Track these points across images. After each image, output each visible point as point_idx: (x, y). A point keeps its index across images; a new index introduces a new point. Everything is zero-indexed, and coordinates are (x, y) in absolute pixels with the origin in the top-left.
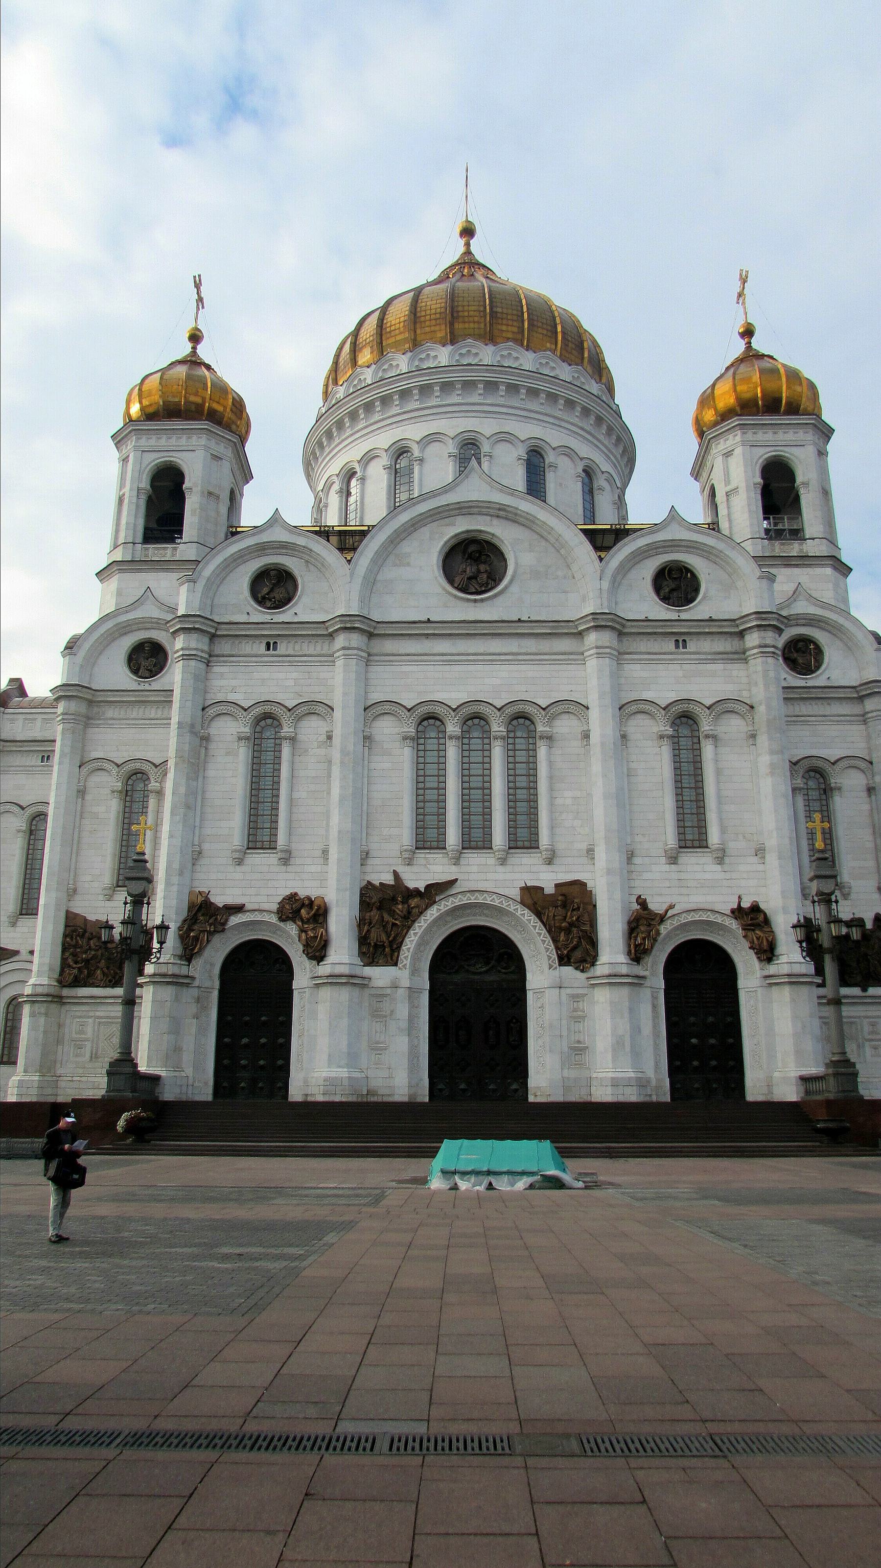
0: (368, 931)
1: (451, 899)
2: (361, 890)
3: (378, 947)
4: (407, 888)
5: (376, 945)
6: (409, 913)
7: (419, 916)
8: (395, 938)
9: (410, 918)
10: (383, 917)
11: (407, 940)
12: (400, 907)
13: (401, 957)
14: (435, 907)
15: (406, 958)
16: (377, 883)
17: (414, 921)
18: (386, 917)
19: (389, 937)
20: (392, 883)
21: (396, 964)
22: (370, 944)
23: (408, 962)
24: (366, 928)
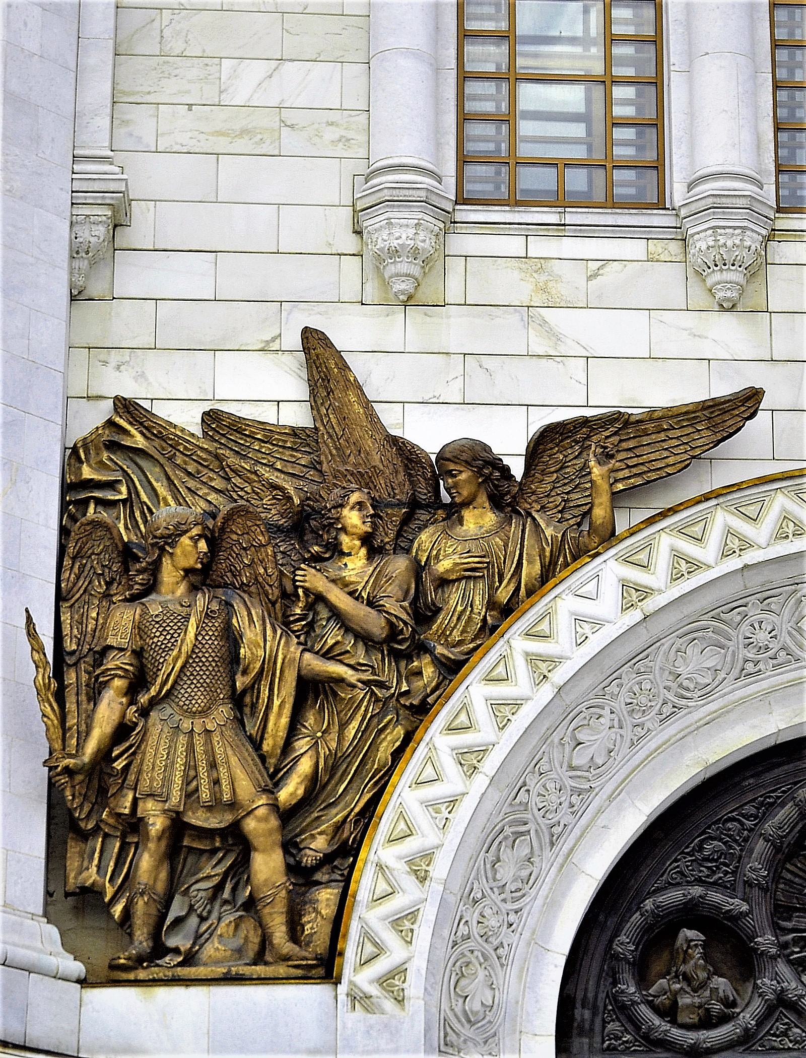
0: (122, 731)
1: (722, 519)
2: (74, 455)
3: (206, 844)
4: (406, 454)
5: (178, 827)
6: (424, 613)
7: (488, 631)
8: (315, 787)
9: (422, 655)
10: (231, 639)
11: (405, 796)
12: (356, 566)
13: (368, 916)
14: (608, 570)
15: (404, 923)
16: (187, 418)
17: (452, 669)
18: (257, 636)
19: (275, 780)
20: (297, 416)
21: (325, 968)
22: (134, 825)
23: (417, 955)
24: (109, 710)
